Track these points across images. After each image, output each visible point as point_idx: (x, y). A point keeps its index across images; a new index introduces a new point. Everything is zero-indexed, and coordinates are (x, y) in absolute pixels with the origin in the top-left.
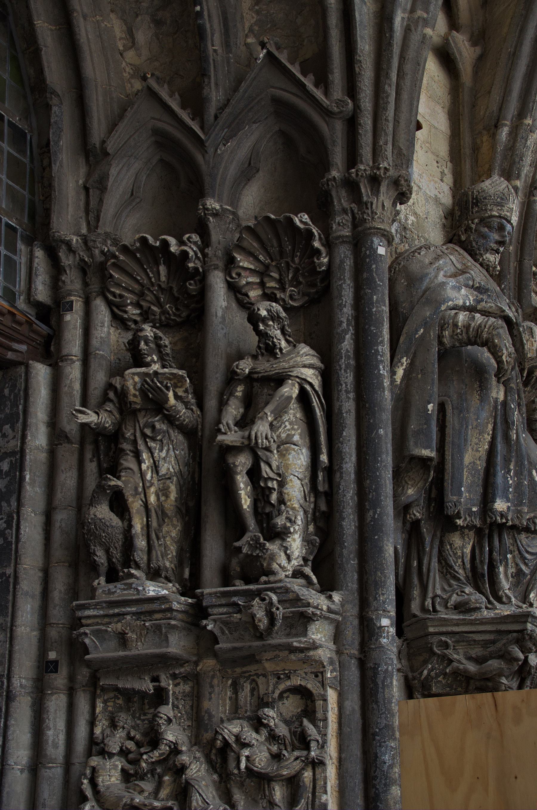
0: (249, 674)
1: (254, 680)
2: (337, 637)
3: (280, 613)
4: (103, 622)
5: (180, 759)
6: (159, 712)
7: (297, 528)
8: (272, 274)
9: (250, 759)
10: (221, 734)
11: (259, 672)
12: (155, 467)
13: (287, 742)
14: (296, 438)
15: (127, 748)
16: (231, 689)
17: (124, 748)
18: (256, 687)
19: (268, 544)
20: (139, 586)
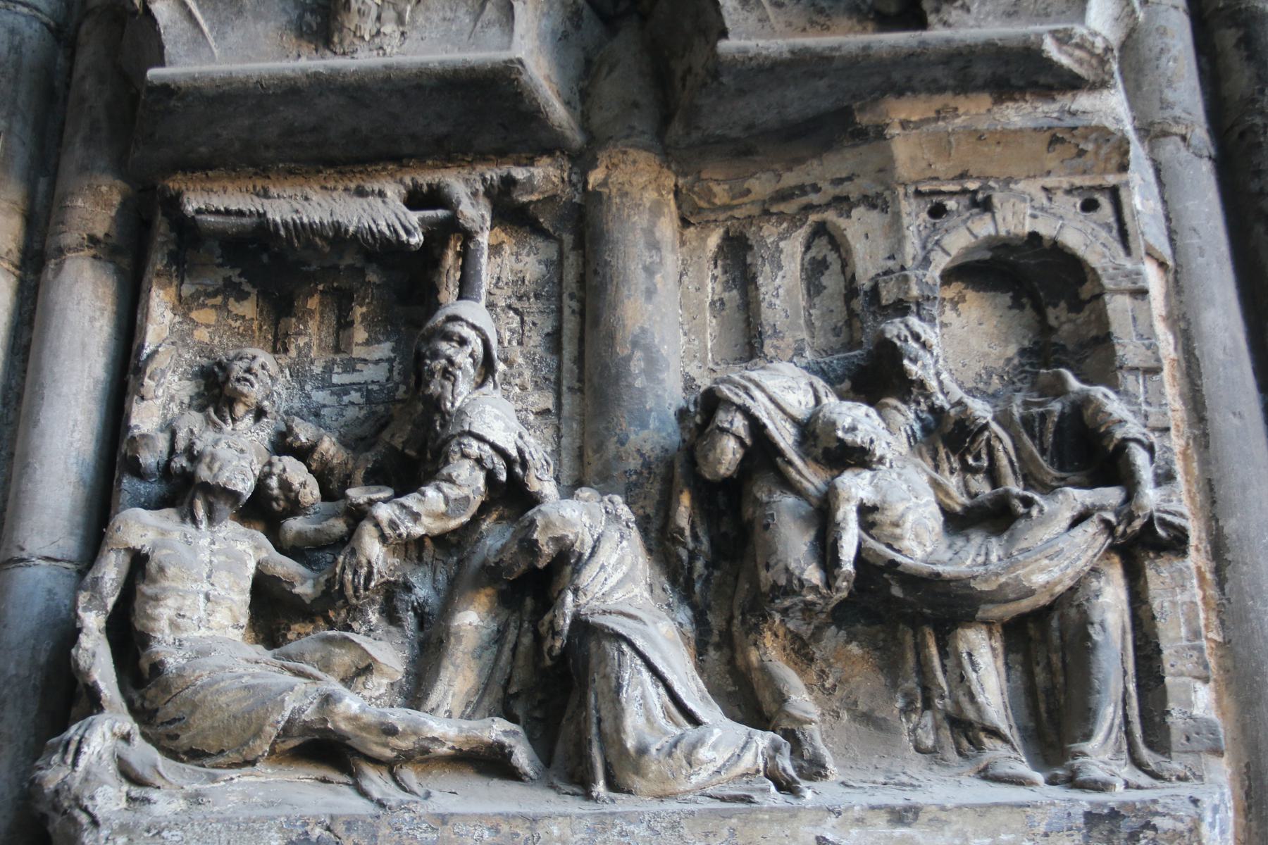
0: (804, 200)
1: (821, 230)
5: (554, 517)
6: (455, 318)
9: (877, 517)
10: (746, 412)
13: (1003, 462)
15: (285, 485)
16: (719, 271)
17: (274, 482)
18: (832, 257)
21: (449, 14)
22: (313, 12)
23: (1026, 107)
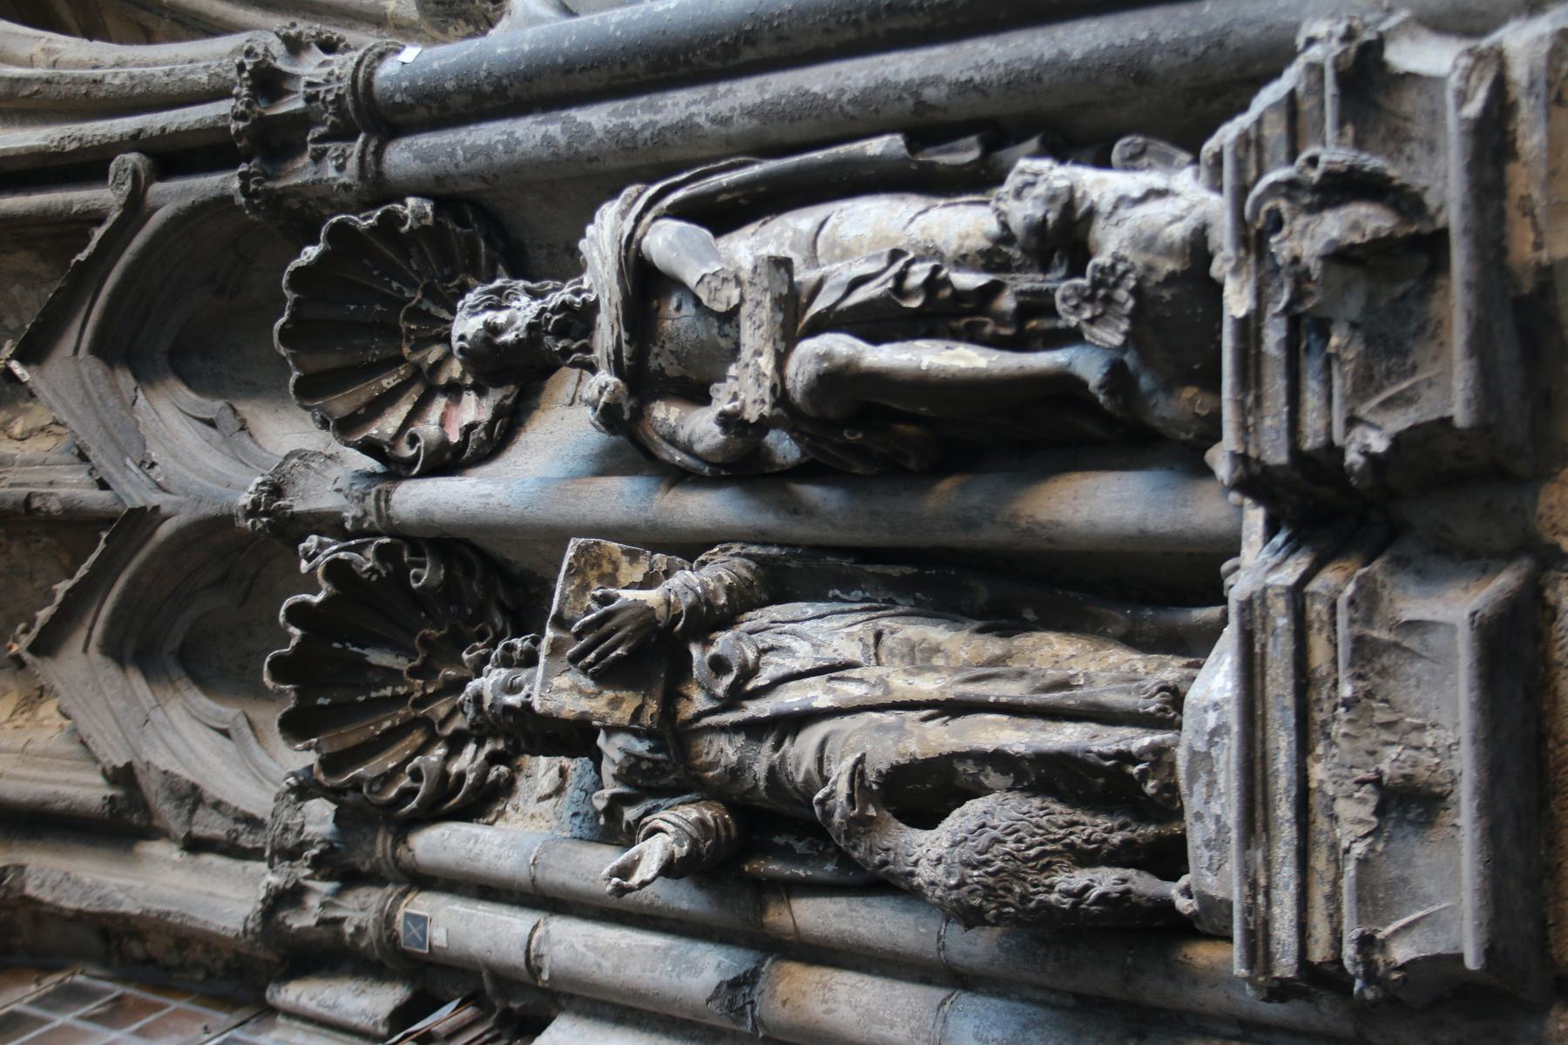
3: (1333, 152)
4: (1330, 875)
12: (833, 670)
19: (1102, 259)
20: (1203, 722)
21: (1413, 682)
22: (1406, 811)
23: (1522, 129)
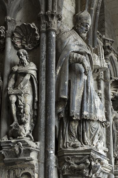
1: (14, 170)
2: (38, 157)
7: (28, 121)
8: (24, 39)
11: (16, 168)
14: (29, 92)
